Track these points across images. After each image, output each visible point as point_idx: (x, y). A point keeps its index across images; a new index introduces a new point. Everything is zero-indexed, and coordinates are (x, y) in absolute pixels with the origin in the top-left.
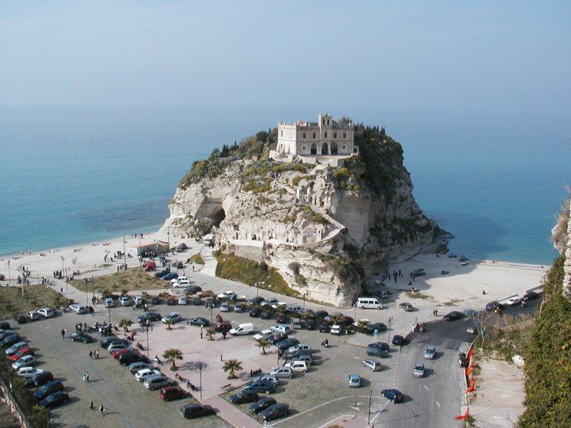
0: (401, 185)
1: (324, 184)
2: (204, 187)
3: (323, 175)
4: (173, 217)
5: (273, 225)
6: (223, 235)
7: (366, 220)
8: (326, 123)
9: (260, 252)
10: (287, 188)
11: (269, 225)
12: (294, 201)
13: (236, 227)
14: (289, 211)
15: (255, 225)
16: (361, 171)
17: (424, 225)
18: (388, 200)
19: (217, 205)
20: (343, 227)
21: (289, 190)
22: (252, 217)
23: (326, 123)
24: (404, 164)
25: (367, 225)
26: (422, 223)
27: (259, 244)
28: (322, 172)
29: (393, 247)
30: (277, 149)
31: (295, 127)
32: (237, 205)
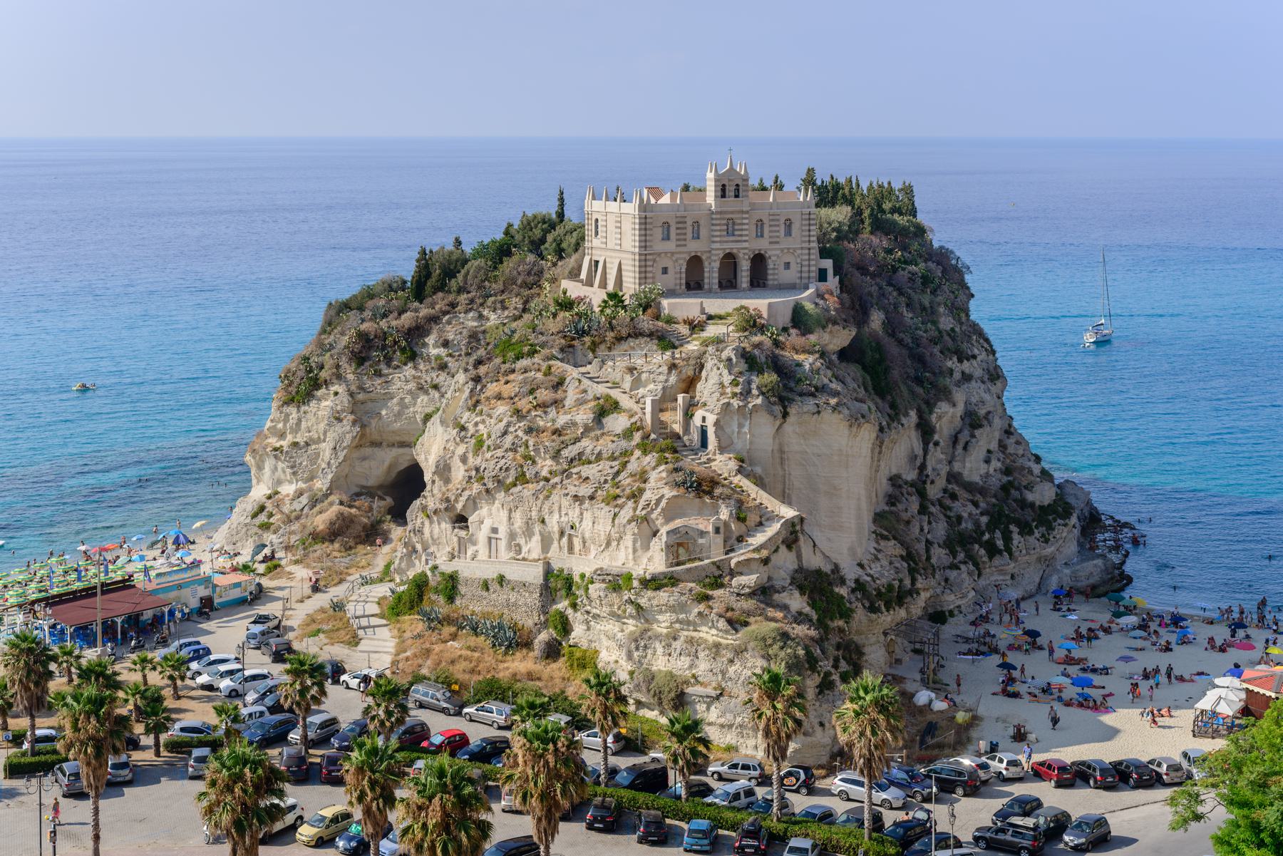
0: (967, 378)
1: (727, 379)
2: (361, 397)
3: (724, 355)
4: (259, 492)
5: (574, 514)
6: (419, 547)
7: (863, 492)
8: (730, 191)
9: (533, 599)
10: (615, 394)
11: (561, 511)
12: (637, 437)
13: (461, 520)
14: (624, 465)
15: (518, 516)
16: (840, 338)
17: (1046, 503)
18: (926, 430)
19: (401, 451)
20: (788, 513)
21: (625, 402)
22: (507, 489)
23: (730, 191)
24: (978, 312)
25: (864, 505)
26: (1043, 495)
27: (534, 574)
28: (718, 341)
29: (953, 574)
30: (583, 276)
31: (631, 208)
32: (461, 450)
